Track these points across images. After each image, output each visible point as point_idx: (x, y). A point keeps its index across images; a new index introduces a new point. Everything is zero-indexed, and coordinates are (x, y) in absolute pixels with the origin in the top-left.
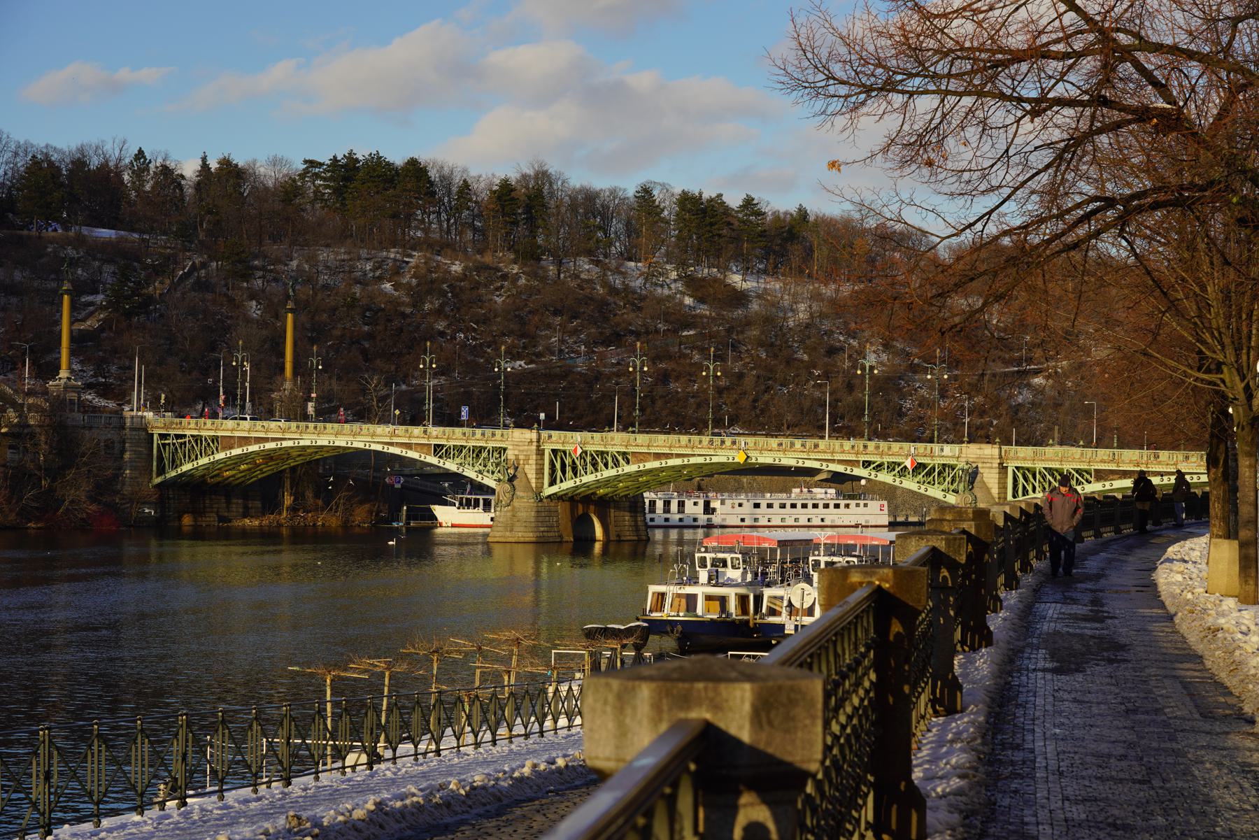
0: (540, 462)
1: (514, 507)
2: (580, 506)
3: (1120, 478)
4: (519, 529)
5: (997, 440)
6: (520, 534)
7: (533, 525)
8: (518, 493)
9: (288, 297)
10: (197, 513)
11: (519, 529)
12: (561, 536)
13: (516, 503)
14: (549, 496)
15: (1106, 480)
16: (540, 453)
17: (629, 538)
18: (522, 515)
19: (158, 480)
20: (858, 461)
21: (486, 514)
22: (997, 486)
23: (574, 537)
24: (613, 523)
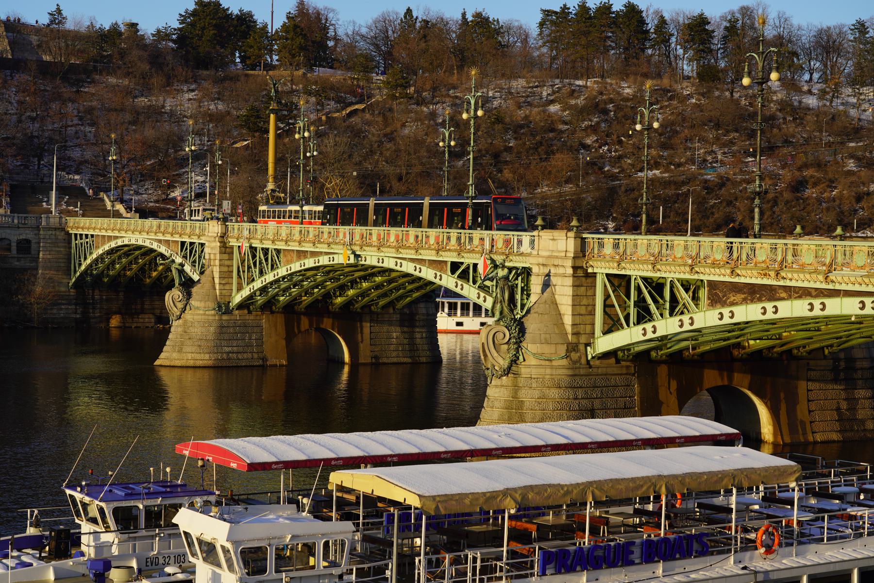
1: (186, 321)
2: (305, 323)
3: (745, 301)
5: (574, 223)
6: (190, 356)
8: (193, 302)
9: (271, 98)
10: (127, 312)
11: (189, 349)
12: (264, 359)
13: (188, 315)
14: (244, 305)
15: (724, 304)
16: (226, 249)
17: (395, 360)
18: (197, 331)
19: (74, 280)
20: (446, 262)
21: (450, 319)
22: (570, 309)
23: (288, 360)
24: (367, 340)
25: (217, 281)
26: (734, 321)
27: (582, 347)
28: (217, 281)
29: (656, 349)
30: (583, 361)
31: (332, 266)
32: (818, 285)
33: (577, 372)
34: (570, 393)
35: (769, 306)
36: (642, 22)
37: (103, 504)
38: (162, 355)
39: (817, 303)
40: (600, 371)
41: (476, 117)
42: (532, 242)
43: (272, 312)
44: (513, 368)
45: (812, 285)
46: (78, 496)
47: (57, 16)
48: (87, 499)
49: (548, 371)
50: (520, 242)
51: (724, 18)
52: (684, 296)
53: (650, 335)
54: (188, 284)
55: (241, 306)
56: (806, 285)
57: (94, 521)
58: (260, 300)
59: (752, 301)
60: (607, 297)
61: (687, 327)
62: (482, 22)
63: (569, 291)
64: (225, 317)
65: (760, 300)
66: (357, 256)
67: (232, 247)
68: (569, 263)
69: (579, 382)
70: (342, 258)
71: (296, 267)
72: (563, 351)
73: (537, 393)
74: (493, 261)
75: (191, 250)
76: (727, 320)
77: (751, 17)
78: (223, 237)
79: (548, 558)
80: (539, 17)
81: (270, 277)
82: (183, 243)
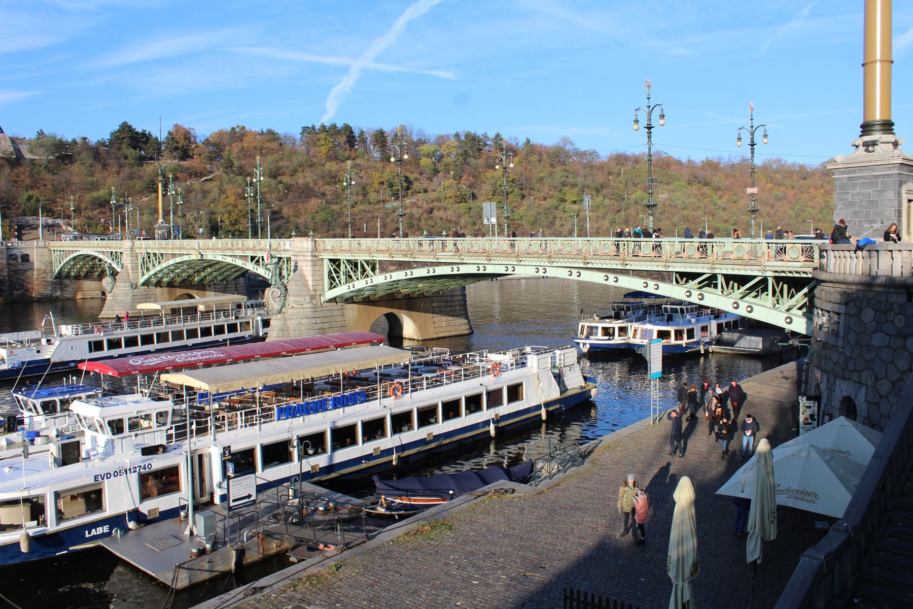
0: (136, 262)
3: (396, 270)
4: (117, 308)
5: (311, 233)
7: (129, 305)
11: (117, 308)
13: (115, 291)
14: (146, 283)
25: (130, 271)
26: (392, 280)
27: (318, 297)
28: (130, 271)
29: (357, 296)
30: (319, 304)
31: (190, 261)
32: (431, 260)
33: (316, 310)
34: (313, 321)
35: (409, 272)
36: (351, 132)
37: (34, 401)
38: (102, 312)
39: (431, 269)
40: (328, 308)
41: (260, 181)
42: (291, 244)
43: (161, 287)
44: (284, 310)
45: (428, 260)
46: (20, 397)
47: (41, 133)
48: (25, 398)
49: (301, 310)
50: (285, 244)
51: (392, 131)
52: (368, 269)
53: (352, 289)
54: (114, 274)
55: (143, 284)
56: (425, 260)
57: (30, 410)
58: (154, 280)
59: (400, 270)
60: (330, 272)
61: (369, 284)
62: (271, 133)
63: (310, 268)
64: (135, 290)
65: (404, 269)
66: (202, 255)
67: (137, 254)
68: (309, 254)
69: (318, 314)
70: (194, 257)
71: (171, 262)
72: (308, 299)
73: (296, 322)
74: (271, 255)
75: (115, 256)
76: (389, 280)
77: (406, 131)
78: (132, 249)
79: (281, 411)
80: (301, 131)
81: (158, 268)
82: (112, 253)
